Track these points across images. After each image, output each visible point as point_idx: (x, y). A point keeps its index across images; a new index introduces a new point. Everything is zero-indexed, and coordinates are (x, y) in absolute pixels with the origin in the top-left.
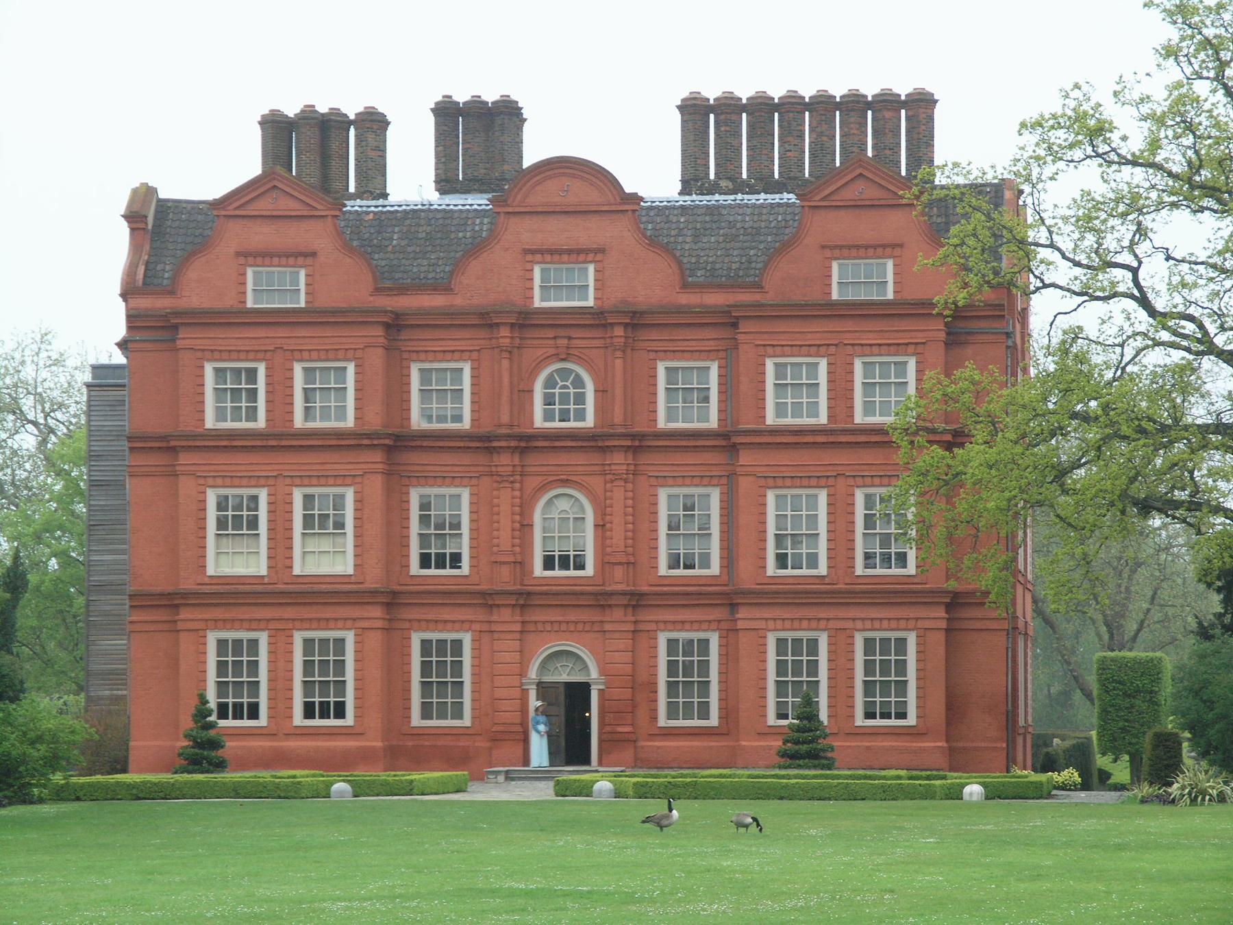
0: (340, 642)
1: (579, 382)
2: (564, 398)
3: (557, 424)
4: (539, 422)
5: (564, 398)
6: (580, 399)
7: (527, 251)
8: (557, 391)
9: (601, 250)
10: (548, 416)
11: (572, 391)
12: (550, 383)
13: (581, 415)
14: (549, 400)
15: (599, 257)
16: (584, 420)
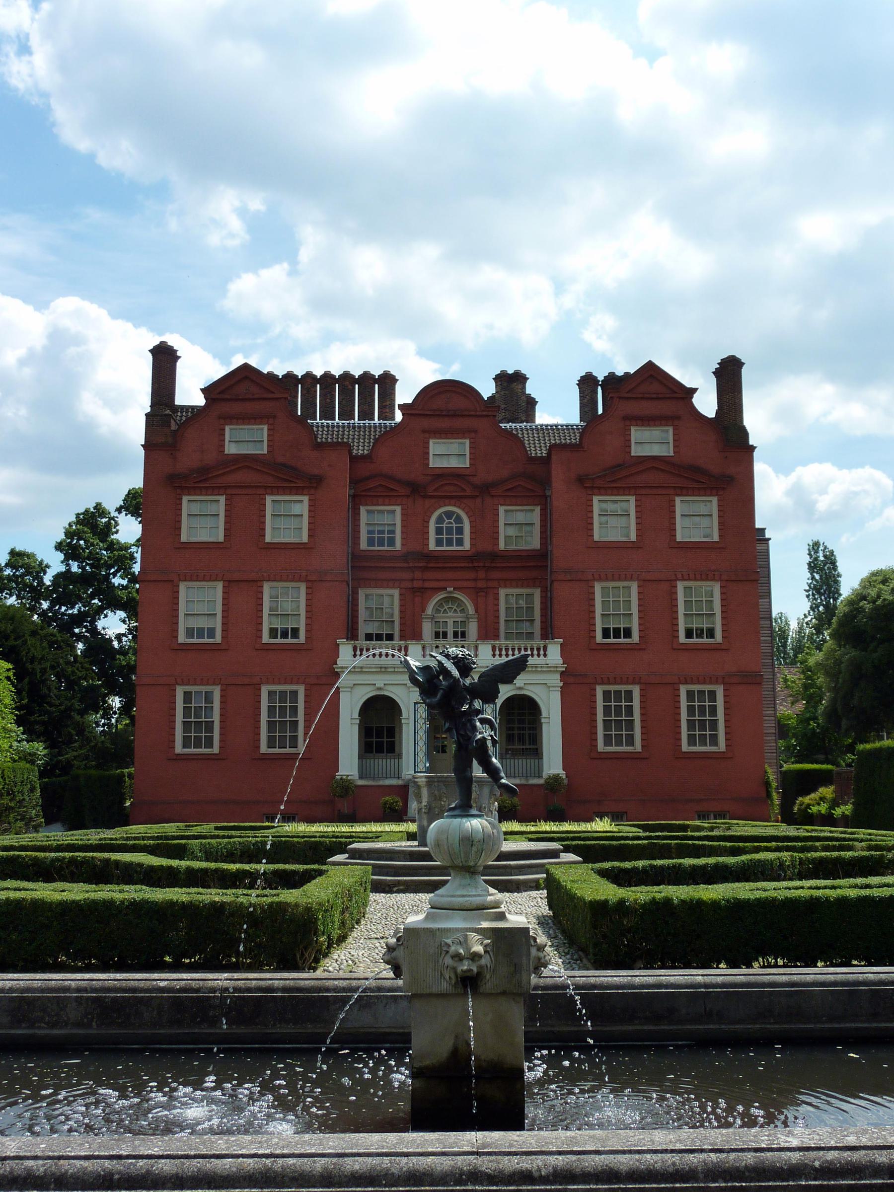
0: (295, 694)
1: (459, 520)
2: (449, 530)
3: (445, 548)
4: (432, 546)
5: (449, 530)
6: (460, 531)
7: (424, 431)
8: (444, 525)
9: (475, 432)
10: (439, 542)
11: (454, 525)
12: (440, 520)
13: (460, 542)
14: (439, 531)
15: (473, 435)
16: (462, 545)
